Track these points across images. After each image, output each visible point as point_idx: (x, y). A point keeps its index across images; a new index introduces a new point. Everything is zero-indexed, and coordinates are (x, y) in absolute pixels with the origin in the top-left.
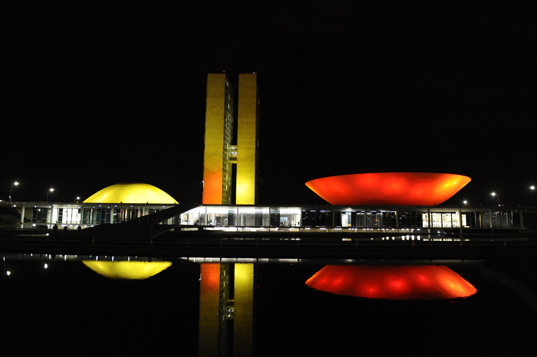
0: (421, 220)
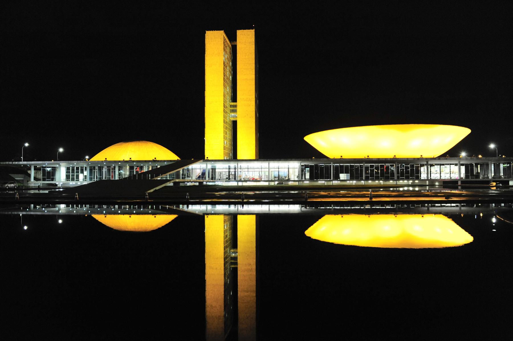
0: (418, 172)
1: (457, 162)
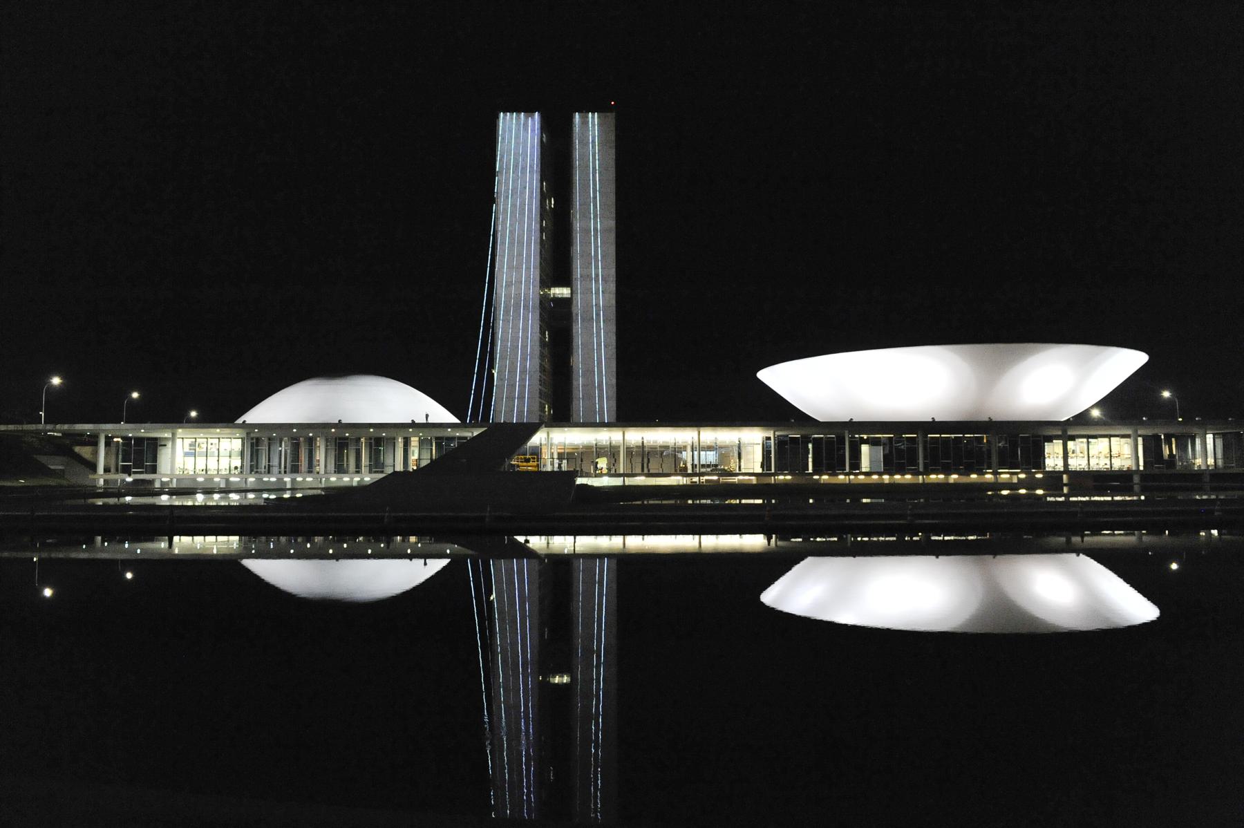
1: (1129, 432)
